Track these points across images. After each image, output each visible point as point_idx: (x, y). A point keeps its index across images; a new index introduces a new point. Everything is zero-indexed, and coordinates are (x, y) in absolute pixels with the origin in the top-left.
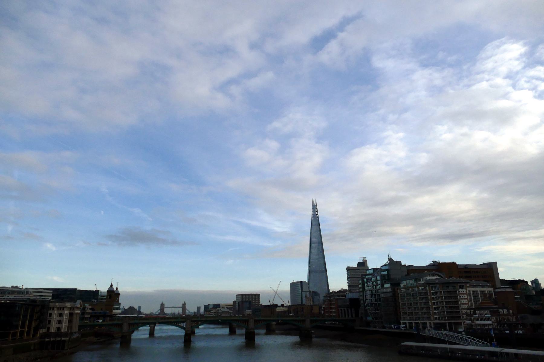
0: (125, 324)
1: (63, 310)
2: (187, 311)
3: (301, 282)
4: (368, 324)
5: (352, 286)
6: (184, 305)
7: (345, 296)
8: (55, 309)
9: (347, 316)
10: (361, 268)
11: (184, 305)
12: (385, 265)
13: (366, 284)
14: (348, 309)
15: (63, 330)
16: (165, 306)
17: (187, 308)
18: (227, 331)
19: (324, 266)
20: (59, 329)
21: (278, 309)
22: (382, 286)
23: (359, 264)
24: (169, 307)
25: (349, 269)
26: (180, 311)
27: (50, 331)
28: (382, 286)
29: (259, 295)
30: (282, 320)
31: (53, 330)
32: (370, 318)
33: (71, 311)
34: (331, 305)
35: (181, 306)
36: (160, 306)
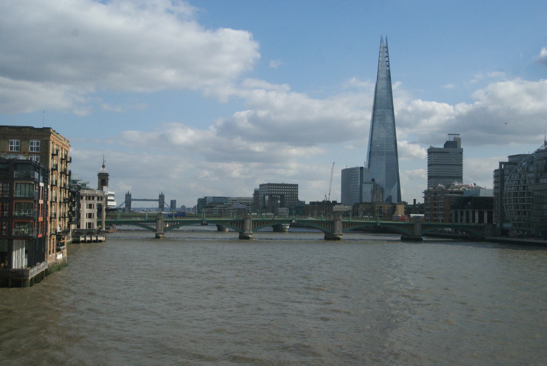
0: (160, 221)
1: (93, 199)
2: (165, 206)
3: (362, 168)
4: (505, 232)
5: (435, 177)
6: (162, 197)
7: (462, 193)
8: (84, 198)
9: (471, 221)
10: (447, 150)
11: (162, 197)
12: (539, 152)
13: (507, 178)
14: (468, 213)
15: (96, 227)
16: (132, 198)
17: (165, 201)
18: (322, 236)
19: (393, 146)
20: (90, 224)
21: (336, 208)
22: (537, 180)
23: (448, 144)
24: (139, 200)
25: (431, 152)
26: (156, 205)
27: (81, 228)
28: (537, 180)
29: (297, 185)
30: (381, 224)
31: (84, 226)
32: (506, 225)
33: (99, 202)
34: (435, 204)
35: (158, 198)
36: (124, 197)
